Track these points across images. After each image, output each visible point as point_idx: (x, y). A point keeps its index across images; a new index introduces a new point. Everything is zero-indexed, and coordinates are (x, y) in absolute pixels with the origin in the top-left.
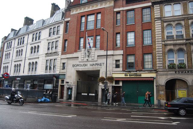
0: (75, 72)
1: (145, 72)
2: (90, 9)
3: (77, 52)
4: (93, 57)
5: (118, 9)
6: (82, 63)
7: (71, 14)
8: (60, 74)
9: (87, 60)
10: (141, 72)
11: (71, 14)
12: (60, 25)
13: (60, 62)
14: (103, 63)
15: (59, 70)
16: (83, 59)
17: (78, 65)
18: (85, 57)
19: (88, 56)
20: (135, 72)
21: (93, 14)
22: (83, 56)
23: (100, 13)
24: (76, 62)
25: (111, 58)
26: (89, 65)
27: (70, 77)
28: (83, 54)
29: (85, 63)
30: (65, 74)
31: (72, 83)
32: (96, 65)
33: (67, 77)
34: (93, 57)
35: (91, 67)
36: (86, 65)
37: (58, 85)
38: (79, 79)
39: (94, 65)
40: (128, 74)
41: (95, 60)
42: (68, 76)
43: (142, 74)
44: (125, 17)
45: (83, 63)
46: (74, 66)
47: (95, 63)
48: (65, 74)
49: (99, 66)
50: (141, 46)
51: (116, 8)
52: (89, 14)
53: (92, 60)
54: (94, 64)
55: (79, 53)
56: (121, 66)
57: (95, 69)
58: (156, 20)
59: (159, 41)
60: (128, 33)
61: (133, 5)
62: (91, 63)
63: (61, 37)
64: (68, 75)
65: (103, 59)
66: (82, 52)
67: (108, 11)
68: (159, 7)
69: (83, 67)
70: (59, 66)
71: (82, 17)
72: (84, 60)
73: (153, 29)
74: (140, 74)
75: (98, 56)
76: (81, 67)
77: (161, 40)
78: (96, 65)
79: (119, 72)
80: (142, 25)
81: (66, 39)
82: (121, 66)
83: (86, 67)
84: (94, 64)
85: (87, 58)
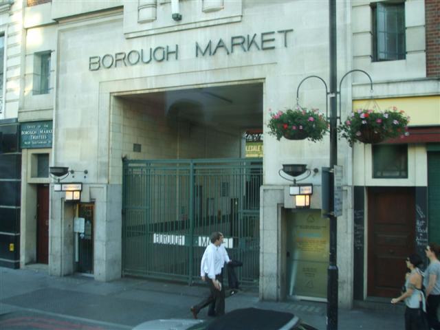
0: (107, 101)
8: (24, 118)
9: (178, 18)
14: (286, 32)
16: (147, 13)
17: (122, 59)
24: (107, 41)
26: (187, 52)
27: (80, 133)
31: (93, 170)
32: (237, 50)
33: (61, 140)
35: (205, 63)
36: (168, 54)
37: (18, 185)
38: (137, 148)
39: (221, 52)
42: (69, 133)
46: (96, 64)
47: (226, 34)
49: (256, 56)
56: (415, 39)
62: (202, 38)
64: (67, 121)
69: (152, 69)
78: (237, 50)
82: (415, 39)
83: (171, 65)
84: (221, 45)
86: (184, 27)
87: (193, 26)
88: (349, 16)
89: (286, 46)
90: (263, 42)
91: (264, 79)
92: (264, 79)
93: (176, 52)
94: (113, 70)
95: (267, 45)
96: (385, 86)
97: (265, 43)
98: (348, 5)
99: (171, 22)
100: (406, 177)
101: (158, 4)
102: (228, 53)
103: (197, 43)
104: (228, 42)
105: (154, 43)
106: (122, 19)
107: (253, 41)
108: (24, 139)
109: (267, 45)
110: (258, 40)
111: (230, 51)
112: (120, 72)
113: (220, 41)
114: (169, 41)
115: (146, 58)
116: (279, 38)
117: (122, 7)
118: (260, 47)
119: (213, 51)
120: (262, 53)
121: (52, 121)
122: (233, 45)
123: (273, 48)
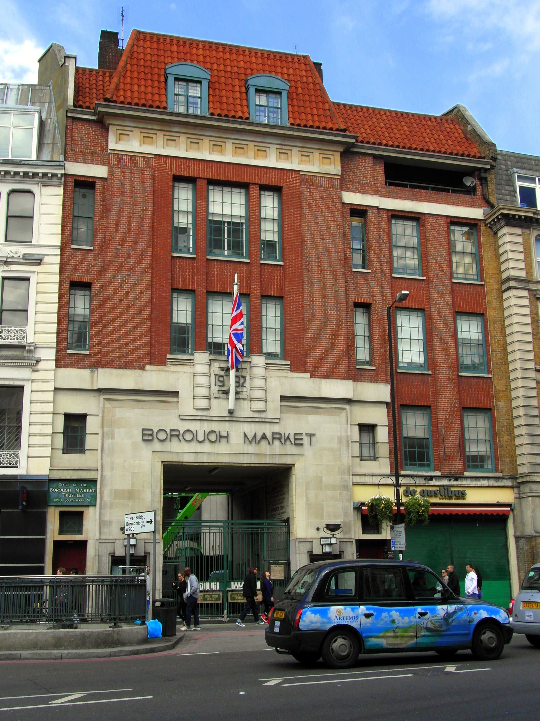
1: (478, 483)
2: (222, 152)
3: (165, 365)
4: (260, 400)
5: (359, 195)
6: (201, 428)
7: (112, 145)
9: (231, 412)
10: (459, 483)
11: (112, 145)
12: (35, 188)
13: (49, 408)
14: (311, 435)
15: (47, 452)
16: (203, 403)
17: (174, 434)
18: (215, 388)
19: (237, 393)
20: (445, 482)
21: (244, 186)
22: (204, 392)
23: (277, 190)
25: (343, 414)
26: (236, 438)
28: (202, 380)
29: (215, 426)
30: (95, 481)
33: (107, 498)
34: (260, 400)
35: (252, 449)
39: (264, 443)
40: (418, 490)
41: (269, 415)
42: (117, 494)
43: (468, 492)
44: (385, 238)
45: (207, 427)
47: (268, 430)
48: (95, 481)
49: (290, 449)
50: (453, 376)
51: (348, 190)
52: (222, 177)
53: (257, 415)
54: (264, 437)
55: (173, 368)
57: (268, 461)
58: (516, 288)
59: (526, 369)
60: (398, 312)
61: (415, 199)
62: (250, 429)
63: (46, 259)
65: (309, 413)
66: (200, 368)
67: (317, 194)
68: (520, 240)
69: (207, 448)
70: (48, 430)
71: (178, 179)
72: (214, 412)
73: (491, 314)
74: (461, 489)
75: (284, 398)
76: (194, 447)
77: (532, 365)
78: (277, 443)
79: (376, 480)
80: (452, 291)
81: (84, 277)
83: (222, 447)
84: (264, 437)
85: (231, 404)
86: (234, 419)
87: (242, 419)
88: (349, 429)
89: (311, 444)
90: (295, 439)
91: (294, 464)
92: (294, 464)
93: (227, 437)
94: (168, 443)
95: (297, 442)
96: (371, 477)
97: (297, 440)
98: (349, 423)
99: (226, 414)
100: (82, 534)
101: (212, 396)
102: (269, 443)
103: (245, 433)
104: (269, 435)
105: (207, 427)
106: (178, 402)
107: (288, 438)
108: (53, 496)
109: (297, 442)
110: (292, 438)
111: (271, 442)
112: (174, 446)
113: (264, 434)
114: (223, 428)
115: (201, 438)
116: (306, 440)
117: (175, 394)
118: (293, 442)
119: (257, 441)
120: (294, 447)
121: (97, 481)
122: (274, 439)
123: (302, 445)
